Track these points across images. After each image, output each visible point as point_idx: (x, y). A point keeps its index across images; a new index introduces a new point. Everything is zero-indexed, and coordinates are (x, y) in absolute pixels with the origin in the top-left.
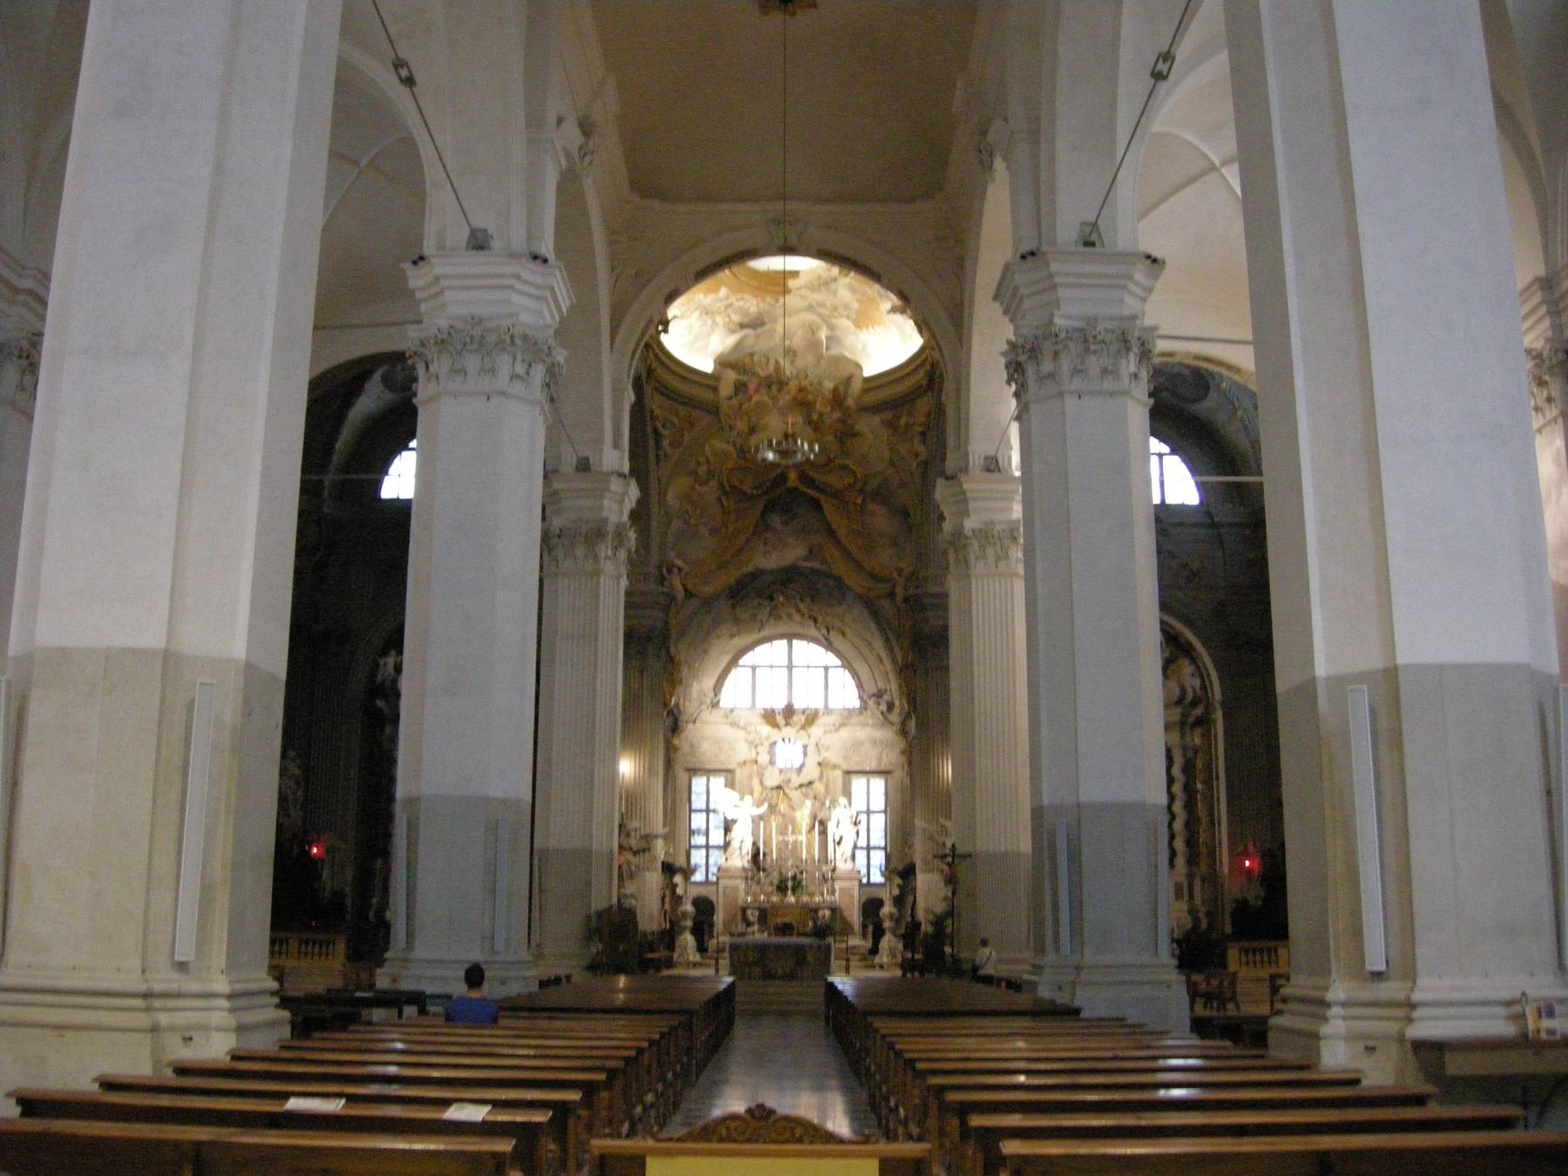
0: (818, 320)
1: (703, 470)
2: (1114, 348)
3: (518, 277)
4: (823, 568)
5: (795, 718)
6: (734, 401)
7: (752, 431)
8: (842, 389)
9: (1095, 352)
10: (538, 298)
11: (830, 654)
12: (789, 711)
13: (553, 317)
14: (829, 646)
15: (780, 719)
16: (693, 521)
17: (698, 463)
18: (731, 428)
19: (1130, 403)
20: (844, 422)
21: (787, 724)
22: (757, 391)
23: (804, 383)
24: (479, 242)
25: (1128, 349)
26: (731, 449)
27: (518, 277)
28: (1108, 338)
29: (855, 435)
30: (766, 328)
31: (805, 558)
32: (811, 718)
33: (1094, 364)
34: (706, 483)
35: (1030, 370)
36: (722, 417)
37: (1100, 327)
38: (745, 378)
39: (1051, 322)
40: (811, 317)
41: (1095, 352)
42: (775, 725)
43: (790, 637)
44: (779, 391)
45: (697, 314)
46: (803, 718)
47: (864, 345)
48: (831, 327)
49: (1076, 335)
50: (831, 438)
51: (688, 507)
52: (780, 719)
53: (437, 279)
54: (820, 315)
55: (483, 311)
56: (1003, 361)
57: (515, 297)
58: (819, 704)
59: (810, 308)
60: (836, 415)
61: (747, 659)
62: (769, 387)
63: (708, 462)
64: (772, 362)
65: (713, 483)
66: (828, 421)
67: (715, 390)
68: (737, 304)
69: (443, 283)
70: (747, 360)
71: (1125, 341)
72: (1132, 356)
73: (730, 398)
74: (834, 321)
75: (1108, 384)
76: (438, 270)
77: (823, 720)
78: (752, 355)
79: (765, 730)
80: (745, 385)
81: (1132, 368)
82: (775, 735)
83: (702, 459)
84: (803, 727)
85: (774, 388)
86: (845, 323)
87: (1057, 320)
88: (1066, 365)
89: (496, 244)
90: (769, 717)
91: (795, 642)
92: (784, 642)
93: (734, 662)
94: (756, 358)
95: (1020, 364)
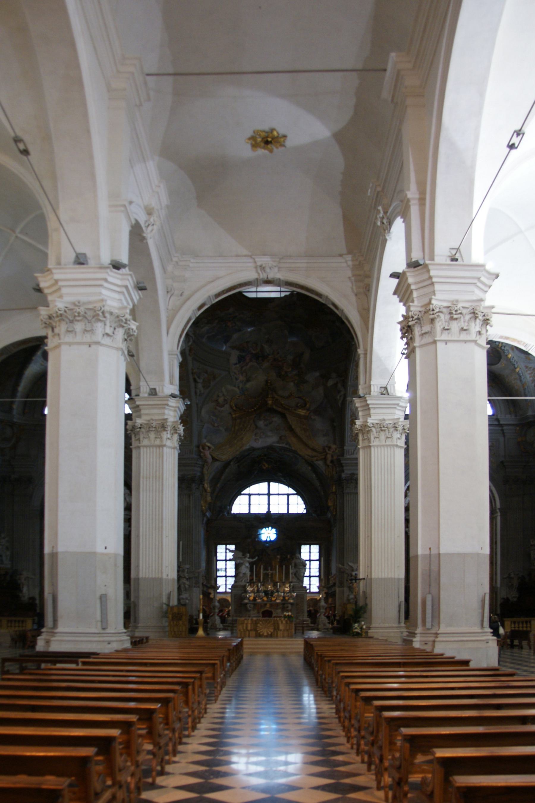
2: (468, 317)
3: (106, 280)
6: (238, 366)
7: (248, 380)
9: (456, 319)
10: (119, 292)
11: (290, 489)
13: (128, 303)
18: (237, 379)
19: (476, 348)
24: (80, 261)
25: (476, 318)
27: (106, 280)
28: (464, 311)
33: (455, 326)
35: (417, 331)
37: (460, 305)
39: (430, 303)
41: (456, 319)
43: (269, 480)
49: (444, 310)
53: (57, 281)
55: (83, 299)
56: (399, 327)
57: (104, 292)
69: (60, 283)
71: (474, 315)
72: (478, 320)
75: (464, 336)
76: (56, 277)
78: (248, 342)
81: (478, 329)
87: (433, 302)
88: (439, 325)
89: (92, 262)
91: (271, 484)
92: (266, 483)
95: (409, 327)
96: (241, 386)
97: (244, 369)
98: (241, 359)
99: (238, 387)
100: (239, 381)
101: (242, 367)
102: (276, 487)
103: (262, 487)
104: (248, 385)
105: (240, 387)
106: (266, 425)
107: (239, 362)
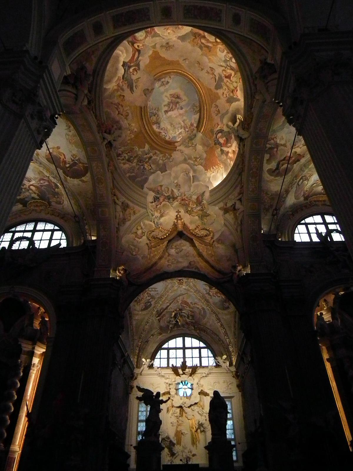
0: (189, 167)
1: (139, 232)
4: (196, 271)
5: (187, 370)
7: (162, 216)
8: (200, 198)
12: (184, 366)
14: (200, 339)
15: (180, 371)
16: (134, 253)
17: (137, 229)
18: (153, 215)
20: (202, 210)
21: (184, 373)
22: (164, 200)
23: (184, 198)
26: (152, 223)
29: (209, 215)
30: (166, 172)
31: (188, 267)
32: (194, 369)
34: (141, 237)
36: (149, 211)
38: (158, 196)
40: (185, 166)
42: (177, 374)
44: (174, 201)
45: (135, 161)
46: (191, 370)
47: (209, 179)
48: (195, 171)
50: (197, 217)
51: (133, 247)
52: (180, 371)
54: (188, 164)
58: (196, 362)
59: (185, 161)
60: (199, 208)
61: (165, 346)
62: (169, 199)
63: (142, 228)
64: (170, 189)
65: (145, 238)
66: (195, 210)
67: (145, 198)
68: (154, 157)
70: (159, 188)
73: (152, 202)
74: (196, 167)
77: (199, 371)
78: (161, 186)
79: (173, 377)
80: (158, 198)
82: (178, 379)
83: (139, 228)
84: (191, 375)
85: (171, 199)
86: (200, 168)
90: (175, 369)
91: (186, 338)
93: (159, 348)
94: (163, 188)
96: (156, 221)
97: (158, 207)
98: (156, 199)
99: (154, 222)
100: (154, 216)
101: (157, 206)
102: (190, 342)
103: (178, 342)
104: (162, 220)
105: (155, 222)
106: (177, 253)
107: (155, 201)
